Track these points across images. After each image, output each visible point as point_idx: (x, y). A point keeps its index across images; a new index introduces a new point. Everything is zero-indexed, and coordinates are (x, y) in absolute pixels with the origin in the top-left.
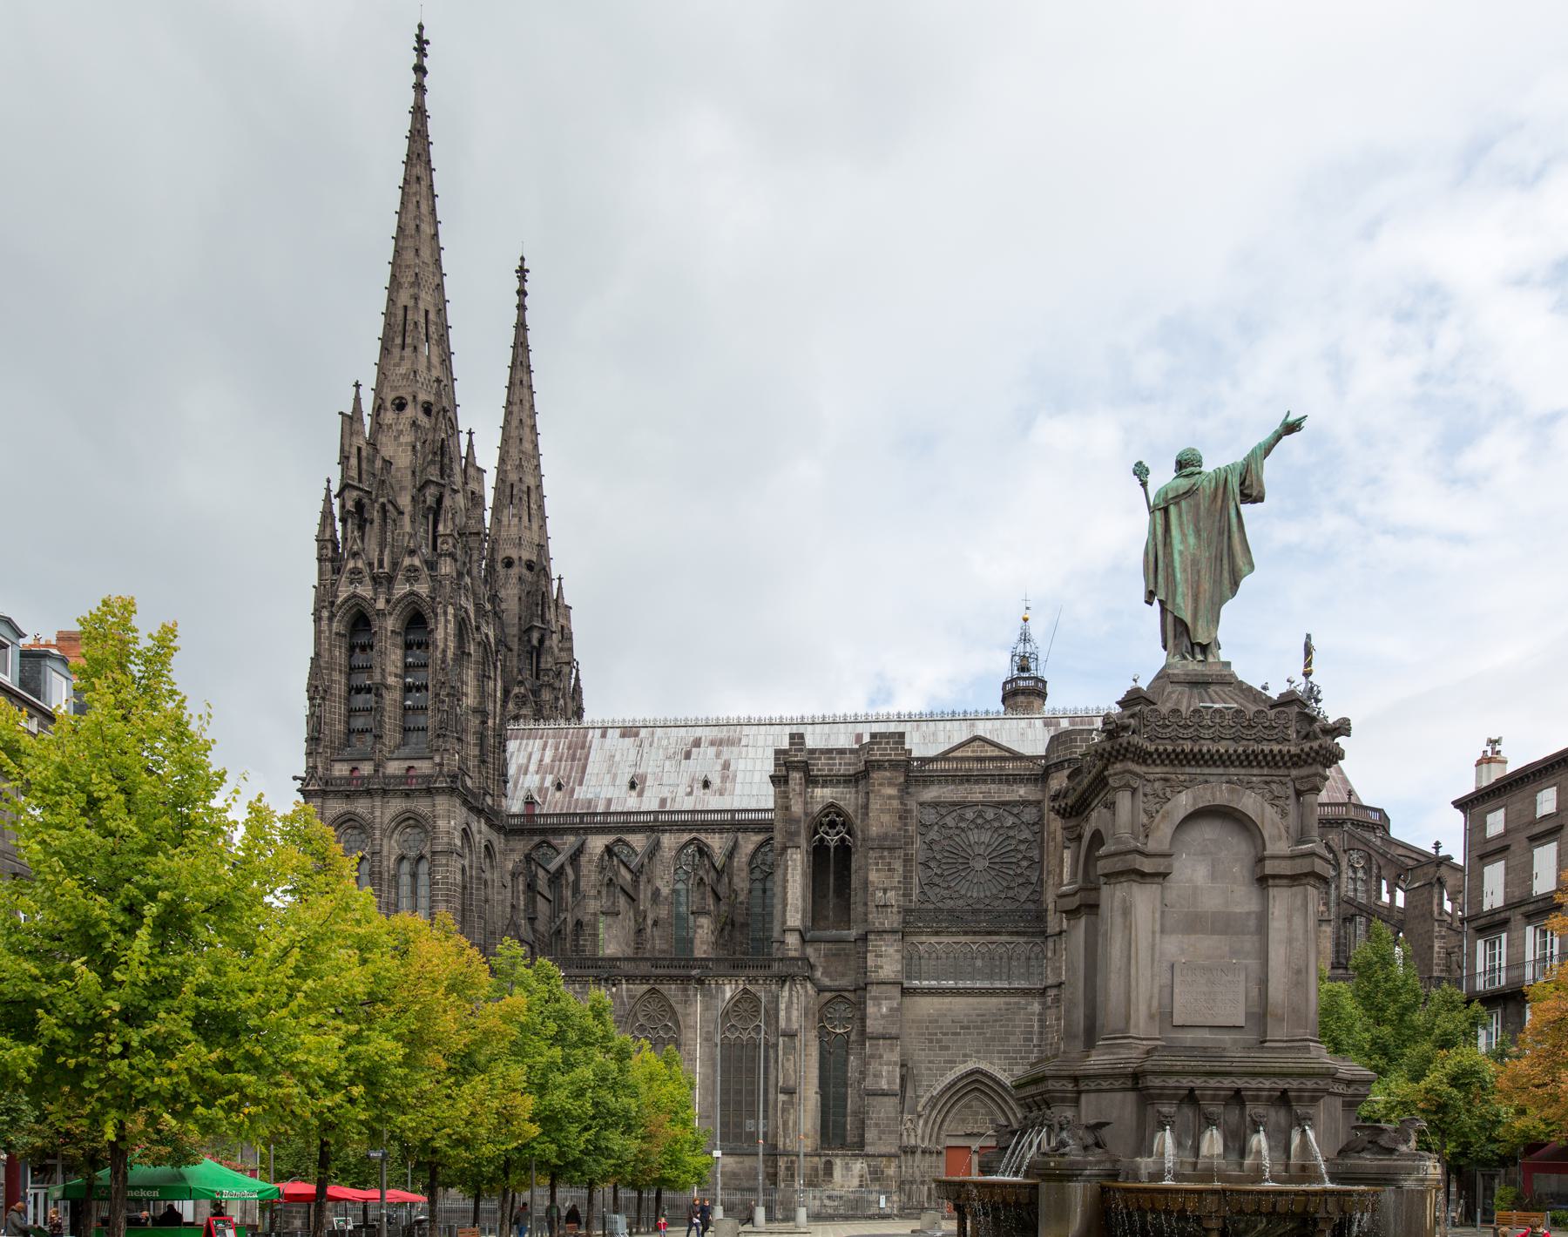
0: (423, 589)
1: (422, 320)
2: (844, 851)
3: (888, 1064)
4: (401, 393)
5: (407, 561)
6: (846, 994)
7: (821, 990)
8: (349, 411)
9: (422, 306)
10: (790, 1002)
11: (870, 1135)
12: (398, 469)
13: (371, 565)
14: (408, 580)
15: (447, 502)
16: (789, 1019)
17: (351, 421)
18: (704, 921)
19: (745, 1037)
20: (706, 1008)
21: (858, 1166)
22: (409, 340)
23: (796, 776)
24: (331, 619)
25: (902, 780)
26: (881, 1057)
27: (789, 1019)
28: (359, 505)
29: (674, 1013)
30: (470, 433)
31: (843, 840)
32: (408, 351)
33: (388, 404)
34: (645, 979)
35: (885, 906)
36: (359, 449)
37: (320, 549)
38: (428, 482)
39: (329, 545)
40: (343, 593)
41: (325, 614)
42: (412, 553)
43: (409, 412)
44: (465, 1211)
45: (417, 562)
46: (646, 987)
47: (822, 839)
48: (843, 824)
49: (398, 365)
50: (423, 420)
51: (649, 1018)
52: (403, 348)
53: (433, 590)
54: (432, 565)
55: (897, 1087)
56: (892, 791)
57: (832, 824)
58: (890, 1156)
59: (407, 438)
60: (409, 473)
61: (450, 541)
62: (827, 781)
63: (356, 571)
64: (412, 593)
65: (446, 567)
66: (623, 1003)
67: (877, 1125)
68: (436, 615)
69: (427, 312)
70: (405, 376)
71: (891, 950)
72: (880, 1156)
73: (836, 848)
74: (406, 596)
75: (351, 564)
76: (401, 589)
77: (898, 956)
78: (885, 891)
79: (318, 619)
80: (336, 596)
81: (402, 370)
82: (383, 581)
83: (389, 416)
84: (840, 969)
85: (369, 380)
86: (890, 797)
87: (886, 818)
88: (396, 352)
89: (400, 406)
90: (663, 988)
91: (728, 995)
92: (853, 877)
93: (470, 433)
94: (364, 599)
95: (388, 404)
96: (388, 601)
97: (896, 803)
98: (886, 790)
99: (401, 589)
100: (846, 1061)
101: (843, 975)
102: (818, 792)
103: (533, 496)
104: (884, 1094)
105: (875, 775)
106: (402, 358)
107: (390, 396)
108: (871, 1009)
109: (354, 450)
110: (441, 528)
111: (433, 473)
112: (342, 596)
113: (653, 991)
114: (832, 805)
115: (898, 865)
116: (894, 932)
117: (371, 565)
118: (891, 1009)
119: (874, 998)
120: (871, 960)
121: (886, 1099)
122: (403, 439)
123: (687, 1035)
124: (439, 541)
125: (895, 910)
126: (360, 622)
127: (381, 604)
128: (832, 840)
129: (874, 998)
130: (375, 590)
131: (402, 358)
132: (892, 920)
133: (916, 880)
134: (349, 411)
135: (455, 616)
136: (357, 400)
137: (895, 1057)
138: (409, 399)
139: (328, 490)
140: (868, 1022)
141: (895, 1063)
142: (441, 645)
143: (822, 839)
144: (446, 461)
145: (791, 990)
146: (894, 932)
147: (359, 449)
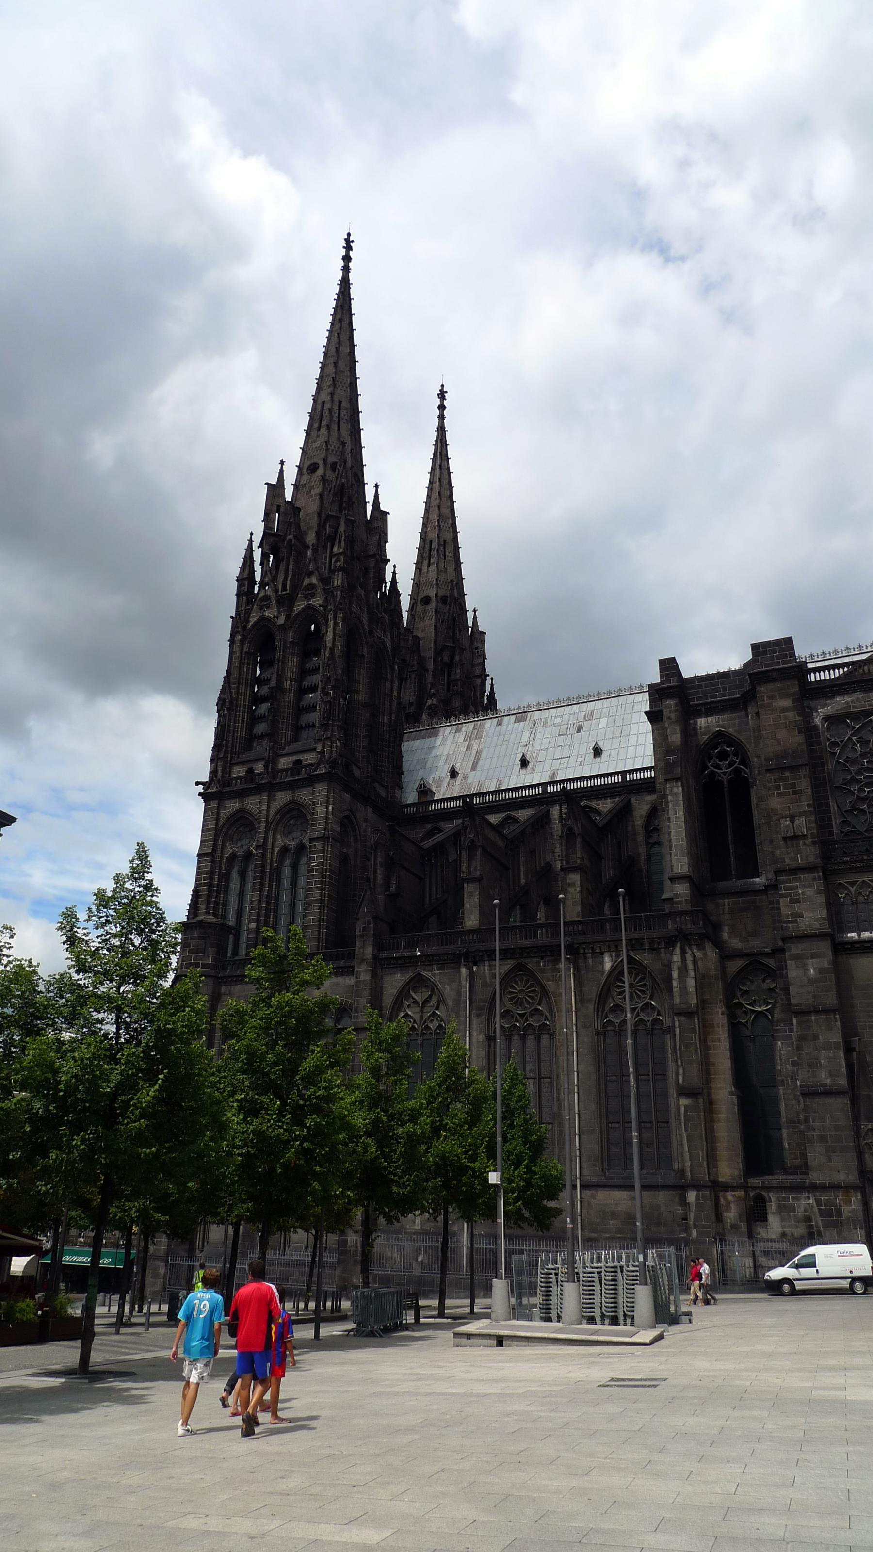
0: (317, 601)
1: (336, 408)
2: (741, 787)
3: (827, 1046)
4: (315, 460)
5: (306, 582)
7: (726, 956)
8: (274, 481)
9: (336, 398)
10: (683, 969)
11: (815, 1155)
12: (307, 515)
13: (276, 591)
14: (307, 597)
15: (342, 528)
17: (275, 490)
18: (575, 878)
20: (579, 984)
21: (806, 1202)
22: (324, 423)
23: (670, 705)
24: (242, 642)
25: (796, 689)
26: (815, 1037)
30: (377, 486)
31: (737, 771)
32: (324, 431)
33: (304, 471)
35: (795, 837)
36: (279, 507)
37: (239, 587)
38: (329, 517)
39: (246, 583)
41: (238, 638)
42: (310, 574)
43: (320, 471)
44: (301, 1264)
45: (314, 580)
47: (713, 772)
48: (736, 754)
49: (315, 441)
50: (330, 475)
52: (319, 429)
53: (326, 600)
54: (326, 581)
55: (843, 1081)
56: (787, 703)
57: (723, 756)
58: (847, 1188)
59: (317, 491)
60: (316, 515)
61: (342, 558)
62: (710, 710)
63: (266, 598)
64: (309, 607)
65: (338, 580)
67: (823, 1139)
68: (327, 620)
69: (340, 402)
70: (319, 448)
71: (810, 892)
72: (835, 1187)
74: (303, 610)
75: (262, 594)
76: (300, 606)
77: (822, 899)
78: (792, 819)
79: (232, 641)
80: (248, 622)
81: (317, 444)
82: (286, 601)
83: (305, 477)
85: (294, 459)
86: (784, 710)
87: (781, 734)
88: (314, 433)
90: (531, 965)
92: (755, 813)
93: (377, 486)
94: (268, 619)
95: (304, 471)
96: (288, 617)
97: (791, 715)
98: (779, 704)
99: (300, 606)
100: (772, 1048)
101: (754, 934)
102: (702, 722)
103: (450, 547)
104: (827, 1093)
105: (762, 689)
106: (318, 436)
107: (307, 463)
108: (793, 972)
109: (275, 508)
110: (335, 549)
111: (333, 511)
112: (253, 620)
115: (804, 784)
116: (809, 869)
117: (276, 591)
118: (821, 971)
120: (785, 910)
121: (830, 1100)
122: (313, 492)
123: (561, 1019)
124: (333, 560)
125: (809, 840)
127: (281, 621)
128: (724, 772)
130: (279, 610)
131: (318, 436)
132: (807, 853)
133: (833, 807)
134: (274, 481)
135: (344, 619)
136: (281, 472)
137: (836, 1037)
138: (321, 463)
139: (251, 541)
140: (793, 990)
141: (836, 1046)
142: (329, 644)
144: (345, 499)
145: (683, 952)
146: (809, 869)
147: (279, 507)
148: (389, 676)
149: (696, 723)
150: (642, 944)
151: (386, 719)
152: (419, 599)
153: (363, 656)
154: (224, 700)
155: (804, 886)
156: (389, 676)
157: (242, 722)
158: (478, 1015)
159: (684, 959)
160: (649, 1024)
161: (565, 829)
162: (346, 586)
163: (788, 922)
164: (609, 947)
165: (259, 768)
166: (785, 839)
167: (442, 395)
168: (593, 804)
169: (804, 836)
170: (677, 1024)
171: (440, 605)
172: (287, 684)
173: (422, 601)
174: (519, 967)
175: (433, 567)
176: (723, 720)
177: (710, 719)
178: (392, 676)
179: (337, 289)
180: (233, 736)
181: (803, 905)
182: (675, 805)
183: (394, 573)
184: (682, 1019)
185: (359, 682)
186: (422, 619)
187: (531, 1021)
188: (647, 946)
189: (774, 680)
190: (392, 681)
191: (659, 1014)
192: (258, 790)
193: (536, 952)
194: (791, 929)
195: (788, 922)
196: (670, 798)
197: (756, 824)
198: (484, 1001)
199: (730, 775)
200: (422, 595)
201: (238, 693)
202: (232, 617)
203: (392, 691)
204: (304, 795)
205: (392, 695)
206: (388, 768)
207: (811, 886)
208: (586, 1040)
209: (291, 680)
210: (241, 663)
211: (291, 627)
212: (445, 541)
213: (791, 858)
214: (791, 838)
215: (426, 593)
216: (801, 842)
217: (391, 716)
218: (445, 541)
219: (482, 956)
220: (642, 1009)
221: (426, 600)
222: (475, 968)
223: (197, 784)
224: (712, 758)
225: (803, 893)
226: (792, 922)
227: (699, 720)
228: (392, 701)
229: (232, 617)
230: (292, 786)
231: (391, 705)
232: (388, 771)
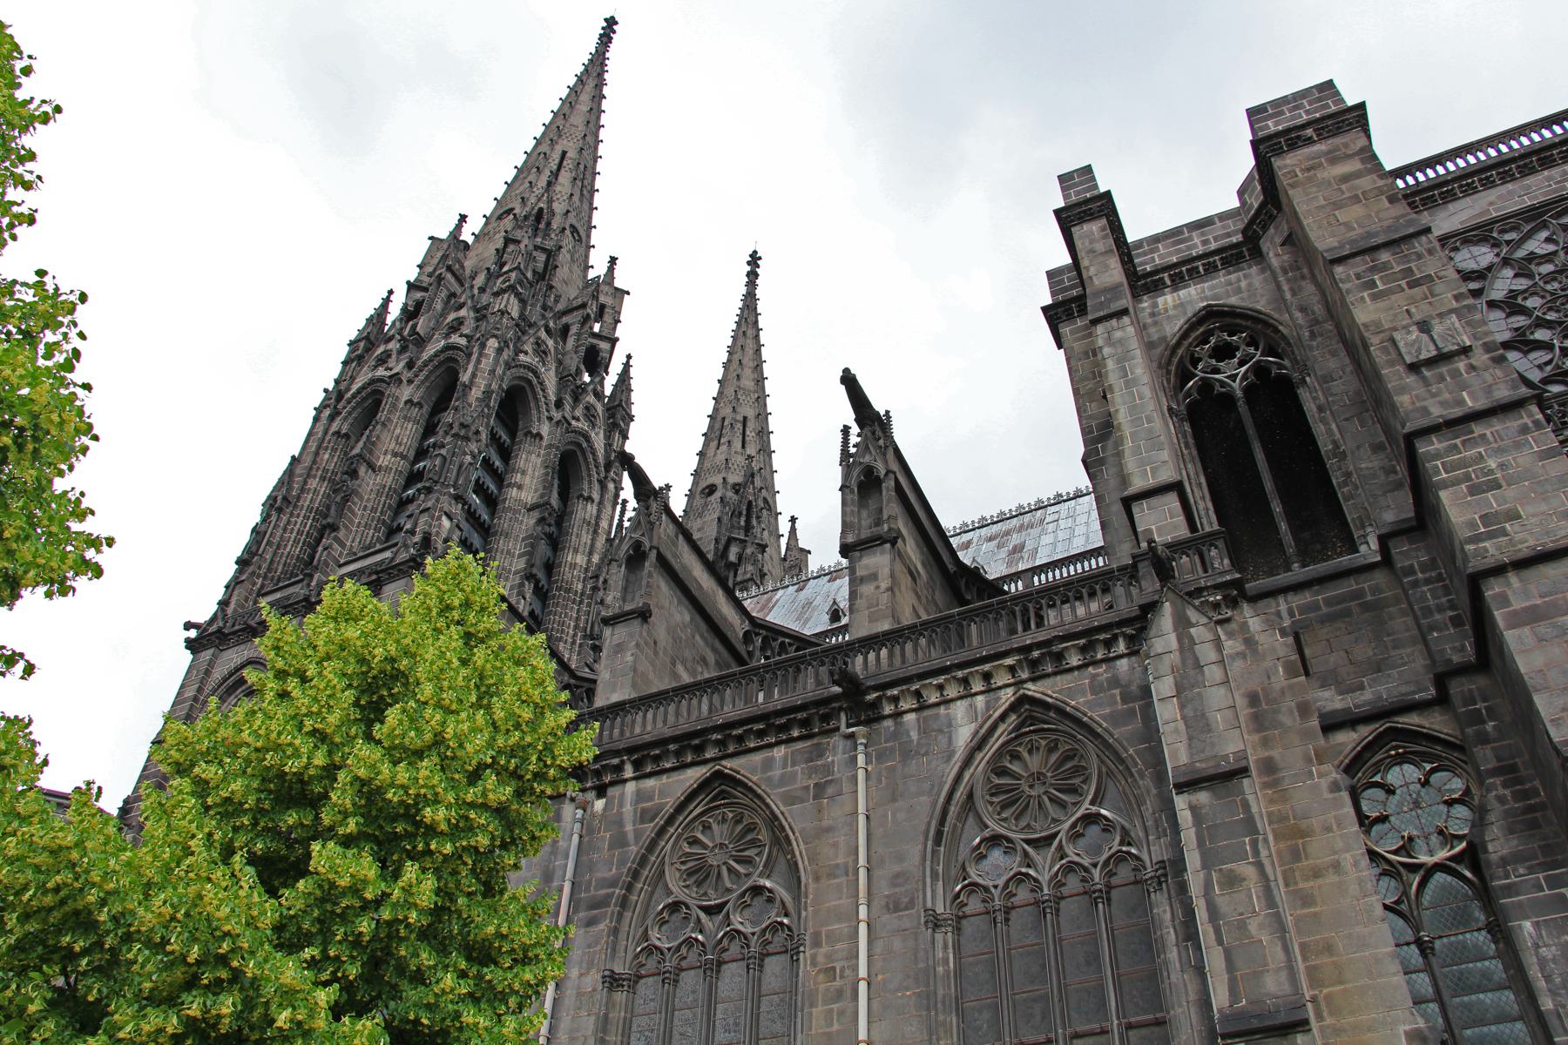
6: (1412, 720)
9: (559, 149)
16: (1197, 725)
19: (1045, 867)
24: (332, 418)
27: (1197, 725)
29: (781, 840)
34: (689, 745)
41: (327, 412)
46: (694, 775)
47: (1206, 386)
48: (1252, 342)
51: (700, 873)
57: (1224, 352)
64: (448, 348)
66: (620, 841)
69: (564, 154)
71: (1523, 459)
73: (1248, 391)
79: (316, 419)
84: (1364, 651)
90: (743, 766)
91: (964, 735)
101: (1378, 667)
102: (1167, 300)
113: (721, 786)
114: (1210, 314)
119: (1531, 616)
123: (822, 899)
128: (1233, 376)
129: (1531, 616)
143: (1206, 386)
148: (596, 496)
149: (1155, 305)
150: (1059, 657)
151: (581, 560)
152: (702, 490)
153: (539, 436)
154: (275, 499)
155: (1500, 451)
156: (596, 496)
157: (300, 533)
158: (591, 922)
159: (1187, 644)
160: (1096, 873)
161: (855, 473)
162: (515, 314)
163: (1477, 539)
164: (965, 681)
166: (1414, 368)
167: (754, 260)
169: (1465, 351)
170: (1185, 816)
171: (730, 494)
172: (384, 460)
173: (702, 492)
175: (724, 448)
176: (1212, 288)
177: (1182, 293)
178: (602, 496)
180: (275, 553)
181: (1510, 493)
182: (1119, 361)
183: (627, 366)
184: (1203, 797)
185: (524, 473)
186: (700, 516)
187: (737, 921)
188: (1075, 660)
189: (1309, 141)
190: (601, 503)
191: (1126, 840)
193: (761, 734)
194: (1492, 551)
195: (1477, 539)
196: (1107, 351)
197: (1325, 446)
198: (613, 883)
199: (1245, 377)
200: (703, 484)
201: (302, 490)
202: (326, 391)
203: (598, 517)
205: (597, 524)
206: (575, 635)
207: (1518, 446)
208: (897, 944)
209: (395, 455)
210: (319, 447)
211: (410, 382)
212: (745, 418)
213: (1443, 404)
214: (1431, 362)
215: (710, 481)
216: (1461, 365)
217: (591, 553)
218: (745, 418)
219: (619, 768)
220: (1075, 836)
221: (711, 489)
222: (599, 804)
223: (188, 626)
224: (1200, 360)
225: (1502, 466)
226: (1491, 535)
227: (1160, 300)
228: (595, 532)
229: (326, 391)
231: (593, 540)
232: (574, 643)
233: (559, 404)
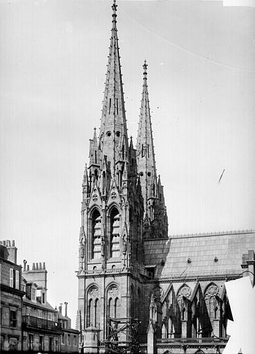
0: (117, 201)
28: (96, 172)
40: (91, 203)
41: (86, 212)
76: (110, 201)
82: (105, 199)
83: (106, 138)
85: (98, 125)
89: (109, 134)
99: (110, 201)
117: (100, 194)
122: (110, 146)
126: (95, 213)
127: (104, 208)
165: (99, 267)
168: (214, 282)
174: (199, 350)
179: (110, 34)
192: (100, 276)
204: (118, 279)
230: (113, 276)
233: (135, 210)
